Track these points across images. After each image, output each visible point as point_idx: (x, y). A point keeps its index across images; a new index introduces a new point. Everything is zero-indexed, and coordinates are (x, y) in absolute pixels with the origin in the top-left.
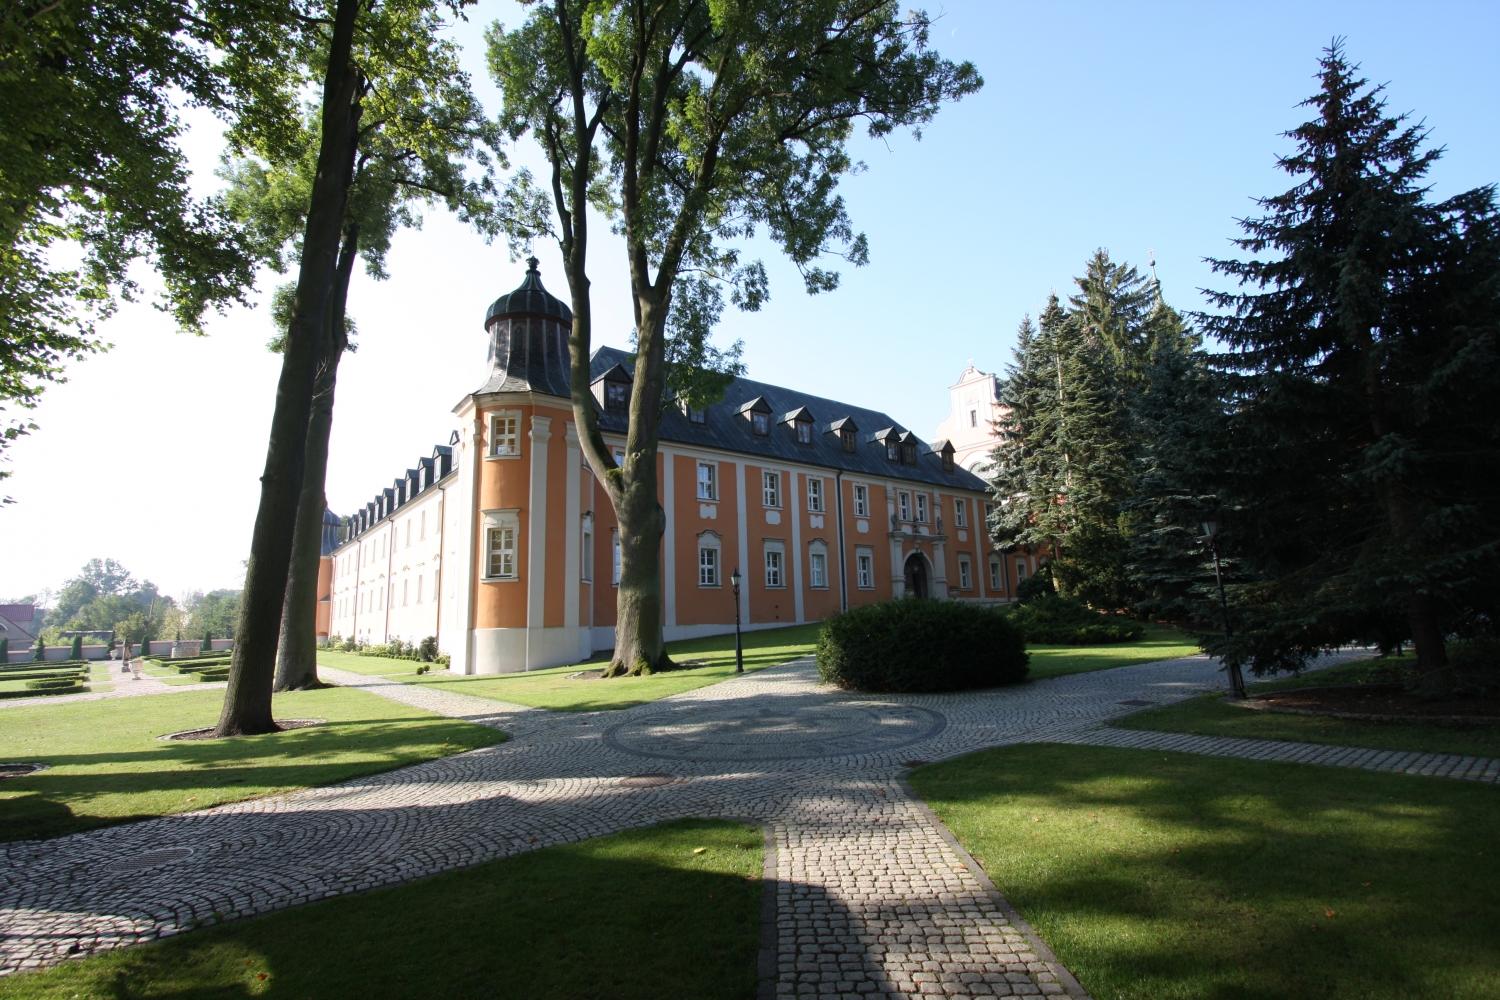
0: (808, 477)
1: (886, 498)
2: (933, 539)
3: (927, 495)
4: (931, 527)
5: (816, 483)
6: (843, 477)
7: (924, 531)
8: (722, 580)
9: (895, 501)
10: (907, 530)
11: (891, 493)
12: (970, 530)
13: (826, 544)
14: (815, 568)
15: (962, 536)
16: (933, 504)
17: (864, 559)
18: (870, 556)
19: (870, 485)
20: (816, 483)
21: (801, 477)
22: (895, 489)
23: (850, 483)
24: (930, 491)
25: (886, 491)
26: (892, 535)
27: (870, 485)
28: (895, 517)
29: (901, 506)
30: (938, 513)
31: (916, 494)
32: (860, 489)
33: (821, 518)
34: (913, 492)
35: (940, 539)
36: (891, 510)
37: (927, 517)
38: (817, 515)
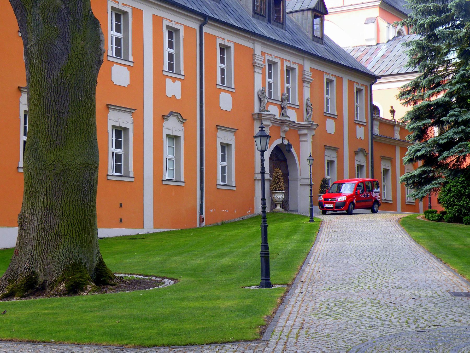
0: (165, 23)
1: (254, 65)
2: (302, 127)
3: (296, 67)
4: (298, 110)
5: (172, 32)
6: (206, 29)
7: (292, 116)
8: (134, 170)
9: (263, 69)
10: (274, 110)
11: (259, 61)
12: (338, 119)
13: (182, 120)
14: (168, 153)
15: (331, 126)
16: (303, 81)
17: (224, 146)
18: (233, 143)
19: (236, 45)
20: (172, 32)
21: (157, 20)
22: (263, 54)
23: (215, 37)
24: (301, 62)
25: (254, 55)
26: (259, 117)
27: (236, 45)
28: (263, 92)
29: (268, 80)
30: (307, 94)
31: (286, 64)
32: (224, 49)
33: (178, 83)
34: (282, 60)
35: (310, 128)
36: (258, 86)
37: (295, 99)
38: (174, 79)
